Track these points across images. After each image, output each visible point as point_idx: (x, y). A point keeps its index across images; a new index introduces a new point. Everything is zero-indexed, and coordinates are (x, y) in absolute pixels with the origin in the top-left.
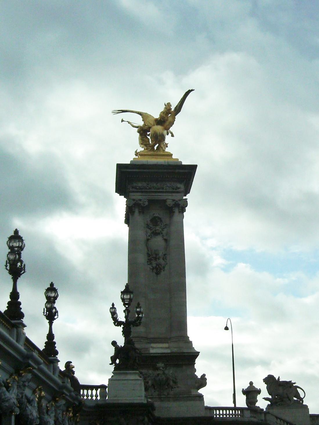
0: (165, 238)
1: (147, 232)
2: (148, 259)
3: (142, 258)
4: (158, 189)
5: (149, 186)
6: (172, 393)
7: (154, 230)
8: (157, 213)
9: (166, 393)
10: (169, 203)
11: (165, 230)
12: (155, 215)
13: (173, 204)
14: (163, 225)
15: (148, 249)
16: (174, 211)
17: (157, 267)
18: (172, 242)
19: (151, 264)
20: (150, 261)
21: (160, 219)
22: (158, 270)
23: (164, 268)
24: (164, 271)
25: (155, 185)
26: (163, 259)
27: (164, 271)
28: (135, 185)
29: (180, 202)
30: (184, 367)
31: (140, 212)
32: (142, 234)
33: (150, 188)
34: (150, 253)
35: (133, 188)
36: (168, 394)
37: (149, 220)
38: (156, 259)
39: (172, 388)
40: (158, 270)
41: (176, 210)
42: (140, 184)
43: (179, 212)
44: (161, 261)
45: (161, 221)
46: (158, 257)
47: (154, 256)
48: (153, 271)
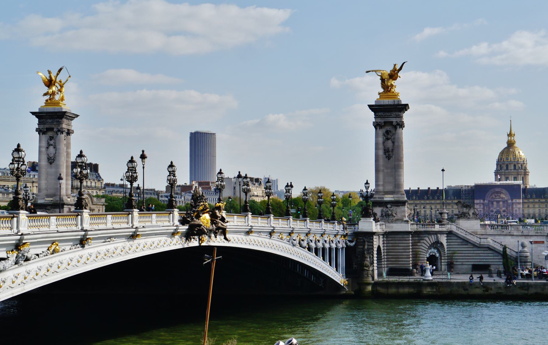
1: (383, 138)
3: (381, 152)
4: (389, 116)
10: (394, 123)
11: (393, 136)
12: (387, 130)
13: (397, 124)
18: (396, 144)
19: (386, 154)
21: (389, 131)
22: (389, 158)
25: (387, 114)
26: (392, 152)
28: (377, 114)
30: (401, 207)
31: (380, 128)
32: (381, 140)
33: (385, 116)
34: (385, 149)
37: (385, 131)
38: (388, 152)
39: (395, 217)
41: (398, 127)
42: (380, 114)
44: (391, 153)
45: (391, 132)
47: (387, 150)
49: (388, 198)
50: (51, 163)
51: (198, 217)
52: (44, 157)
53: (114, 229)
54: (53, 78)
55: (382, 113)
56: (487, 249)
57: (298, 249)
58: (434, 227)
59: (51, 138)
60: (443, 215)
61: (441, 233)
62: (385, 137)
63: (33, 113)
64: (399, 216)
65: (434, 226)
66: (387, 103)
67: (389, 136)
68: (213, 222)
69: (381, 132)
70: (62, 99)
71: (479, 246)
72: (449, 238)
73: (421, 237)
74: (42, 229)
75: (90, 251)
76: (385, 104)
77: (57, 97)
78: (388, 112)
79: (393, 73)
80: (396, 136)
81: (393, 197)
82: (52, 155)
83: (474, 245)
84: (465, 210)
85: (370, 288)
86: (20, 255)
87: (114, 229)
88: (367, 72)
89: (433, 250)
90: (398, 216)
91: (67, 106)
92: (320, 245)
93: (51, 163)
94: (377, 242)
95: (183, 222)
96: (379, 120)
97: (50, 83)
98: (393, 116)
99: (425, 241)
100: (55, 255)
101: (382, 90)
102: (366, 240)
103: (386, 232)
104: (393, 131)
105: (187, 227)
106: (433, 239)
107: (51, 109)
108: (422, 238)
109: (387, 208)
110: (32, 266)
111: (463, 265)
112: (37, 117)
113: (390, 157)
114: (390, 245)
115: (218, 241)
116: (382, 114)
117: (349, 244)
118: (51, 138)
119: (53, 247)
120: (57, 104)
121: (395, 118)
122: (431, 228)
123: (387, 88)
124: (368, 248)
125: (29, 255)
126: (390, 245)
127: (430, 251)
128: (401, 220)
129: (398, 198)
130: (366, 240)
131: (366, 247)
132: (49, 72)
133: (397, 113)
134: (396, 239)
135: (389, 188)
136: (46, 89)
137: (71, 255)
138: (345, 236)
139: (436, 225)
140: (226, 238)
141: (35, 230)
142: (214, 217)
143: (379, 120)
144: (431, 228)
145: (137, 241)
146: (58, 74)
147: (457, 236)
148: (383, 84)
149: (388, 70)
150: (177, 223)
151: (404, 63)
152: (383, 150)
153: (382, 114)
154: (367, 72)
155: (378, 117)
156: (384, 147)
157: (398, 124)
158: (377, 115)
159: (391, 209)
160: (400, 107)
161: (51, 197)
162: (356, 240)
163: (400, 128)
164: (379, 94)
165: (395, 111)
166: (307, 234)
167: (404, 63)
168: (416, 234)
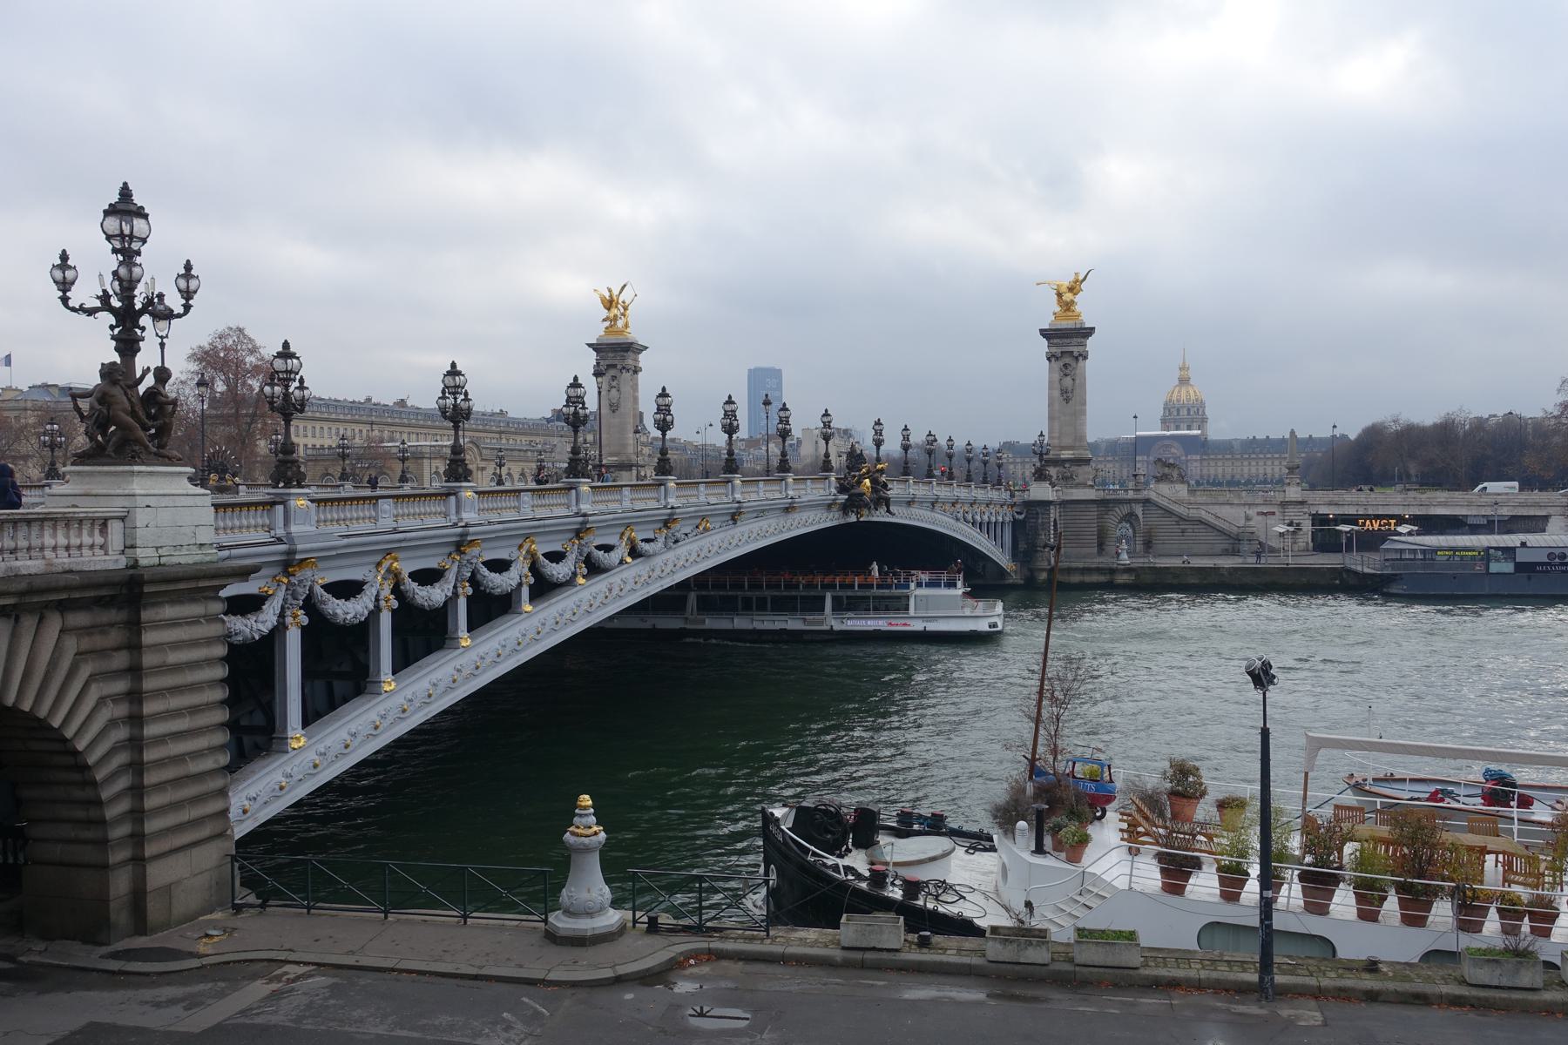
3: (1057, 393)
10: (1076, 354)
18: (1077, 382)
22: (1067, 400)
28: (1052, 341)
32: (1057, 376)
40: (1067, 400)
41: (1081, 358)
42: (1055, 341)
44: (1070, 394)
49: (1066, 454)
50: (614, 412)
51: (859, 483)
52: (605, 403)
53: (767, 499)
54: (615, 298)
56: (1198, 523)
57: (961, 526)
59: (614, 378)
61: (1137, 501)
63: (589, 345)
64: (1080, 479)
68: (874, 490)
69: (1057, 365)
70: (626, 326)
71: (1186, 518)
72: (1146, 508)
74: (693, 500)
75: (742, 529)
77: (620, 323)
78: (1067, 338)
81: (1073, 454)
82: (614, 401)
83: (1181, 519)
84: (1166, 470)
86: (670, 535)
87: (767, 499)
88: (1038, 284)
89: (1124, 524)
91: (635, 334)
92: (986, 518)
93: (614, 412)
94: (1054, 513)
95: (842, 489)
96: (1054, 350)
97: (609, 303)
100: (706, 534)
101: (1058, 309)
102: (1039, 511)
103: (1063, 501)
104: (1074, 364)
105: (847, 497)
106: (1125, 509)
107: (613, 339)
109: (1065, 468)
110: (683, 550)
111: (1163, 543)
112: (594, 349)
114: (1069, 517)
115: (880, 516)
117: (1017, 516)
118: (614, 378)
119: (703, 525)
120: (621, 332)
123: (1067, 306)
125: (678, 535)
126: (1069, 517)
127: (1120, 526)
128: (1084, 485)
129: (1079, 454)
131: (1040, 521)
132: (610, 290)
133: (1079, 340)
134: (1078, 510)
135: (1067, 441)
136: (605, 313)
137: (722, 535)
138: (1012, 506)
140: (888, 511)
141: (684, 501)
142: (874, 481)
143: (1054, 350)
145: (796, 517)
146: (620, 293)
147: (1157, 506)
149: (1066, 283)
150: (834, 491)
154: (1038, 284)
157: (1080, 355)
161: (616, 456)
162: (1027, 512)
164: (1055, 314)
166: (987, 505)
168: (1103, 504)
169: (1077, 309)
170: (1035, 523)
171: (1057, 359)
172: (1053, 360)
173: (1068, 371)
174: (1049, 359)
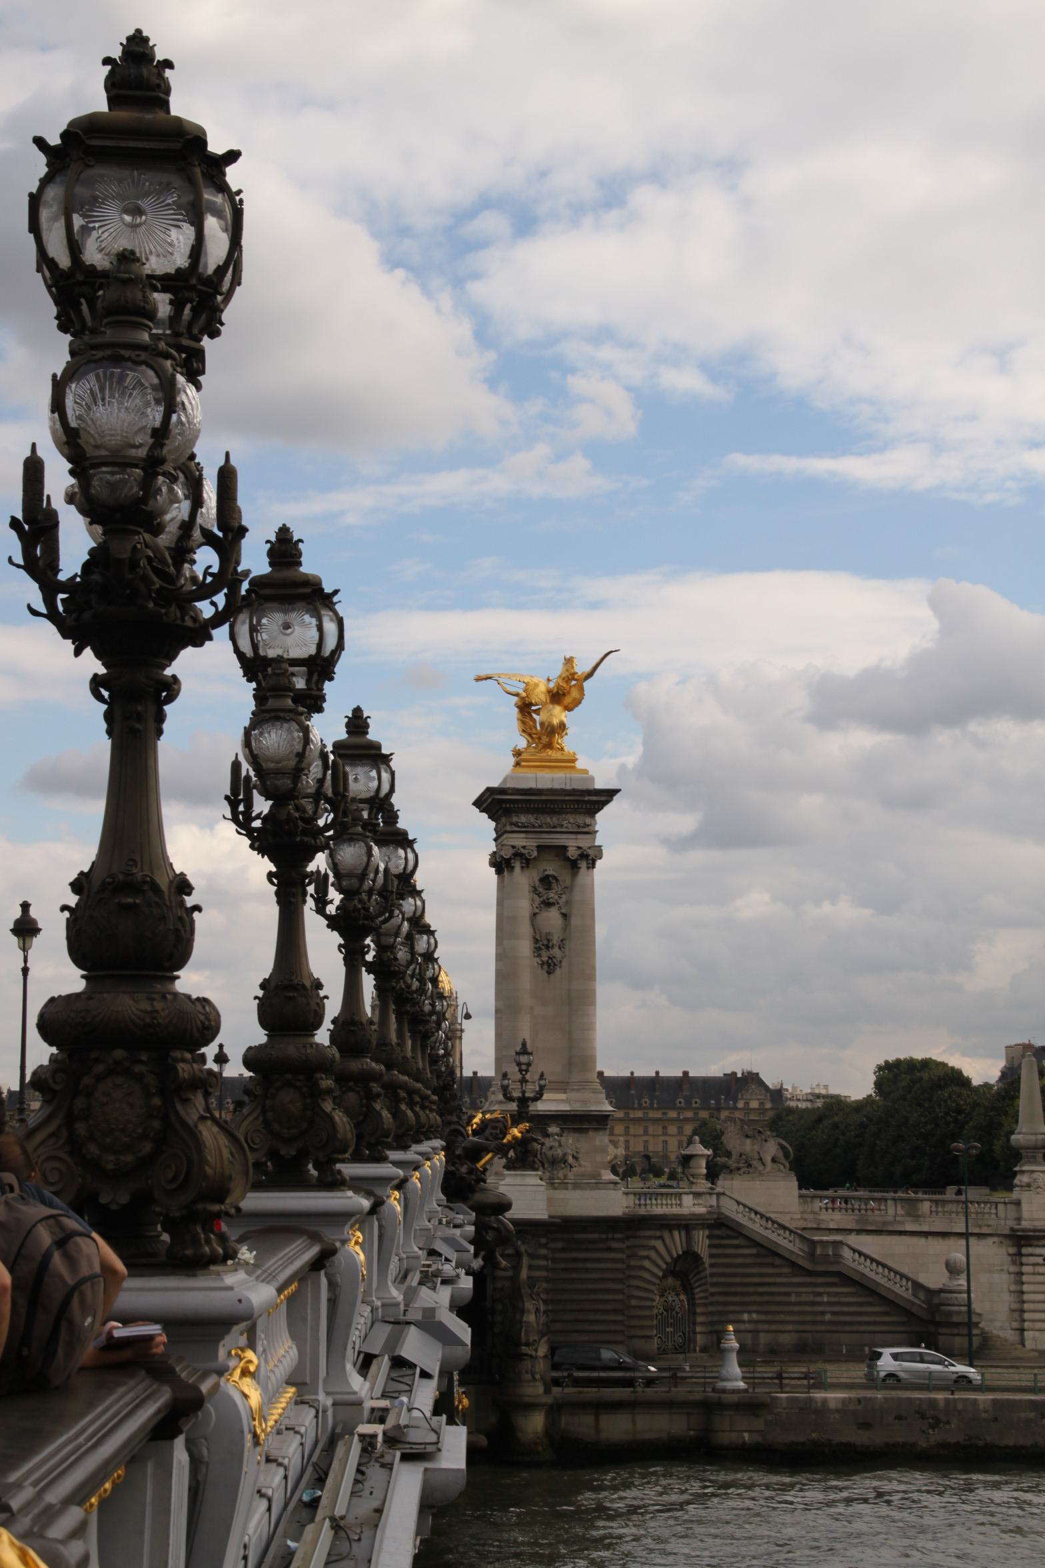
0: (564, 911)
1: (533, 900)
2: (536, 948)
3: (525, 948)
4: (555, 827)
5: (539, 822)
6: (571, 1175)
7: (545, 898)
8: (551, 867)
9: (561, 1175)
10: (572, 853)
11: (564, 896)
12: (547, 873)
13: (579, 855)
14: (560, 889)
15: (534, 929)
16: (580, 866)
17: (550, 961)
18: (575, 921)
19: (539, 956)
20: (537, 951)
21: (555, 878)
22: (550, 966)
23: (561, 961)
24: (560, 967)
25: (548, 820)
26: (560, 948)
27: (560, 967)
28: (515, 819)
29: (590, 852)
30: (591, 1133)
31: (522, 868)
32: (524, 905)
33: (540, 826)
34: (538, 938)
35: (512, 824)
36: (565, 1177)
38: (547, 947)
39: (571, 1167)
41: (583, 865)
42: (523, 819)
43: (588, 868)
44: (556, 952)
45: (557, 880)
46: (551, 945)
47: (545, 942)
48: (542, 968)
55: (530, 816)
58: (678, 1202)
60: (692, 1163)
62: (536, 897)
65: (680, 1199)
66: (548, 786)
67: (552, 895)
69: (522, 879)
73: (640, 1237)
76: (540, 786)
78: (552, 812)
79: (564, 685)
80: (577, 896)
85: (535, 1423)
90: (582, 1163)
96: (519, 840)
98: (566, 827)
99: (652, 1254)
101: (522, 743)
102: (523, 1248)
104: (565, 877)
106: (677, 1244)
108: (645, 1242)
109: (547, 1135)
113: (555, 965)
116: (532, 820)
121: (573, 836)
122: (671, 1205)
124: (528, 1277)
129: (584, 1102)
130: (526, 1251)
131: (524, 1274)
133: (582, 819)
139: (685, 1197)
143: (519, 840)
144: (671, 1205)
148: (527, 720)
151: (611, 652)
152: (532, 939)
153: (532, 820)
154: (478, 679)
155: (516, 829)
156: (535, 932)
157: (584, 856)
158: (516, 825)
159: (563, 1139)
160: (595, 798)
163: (588, 868)
165: (575, 811)
167: (611, 652)
169: (569, 743)
170: (511, 1279)
171: (527, 863)
172: (517, 865)
173: (552, 895)
174: (500, 864)
